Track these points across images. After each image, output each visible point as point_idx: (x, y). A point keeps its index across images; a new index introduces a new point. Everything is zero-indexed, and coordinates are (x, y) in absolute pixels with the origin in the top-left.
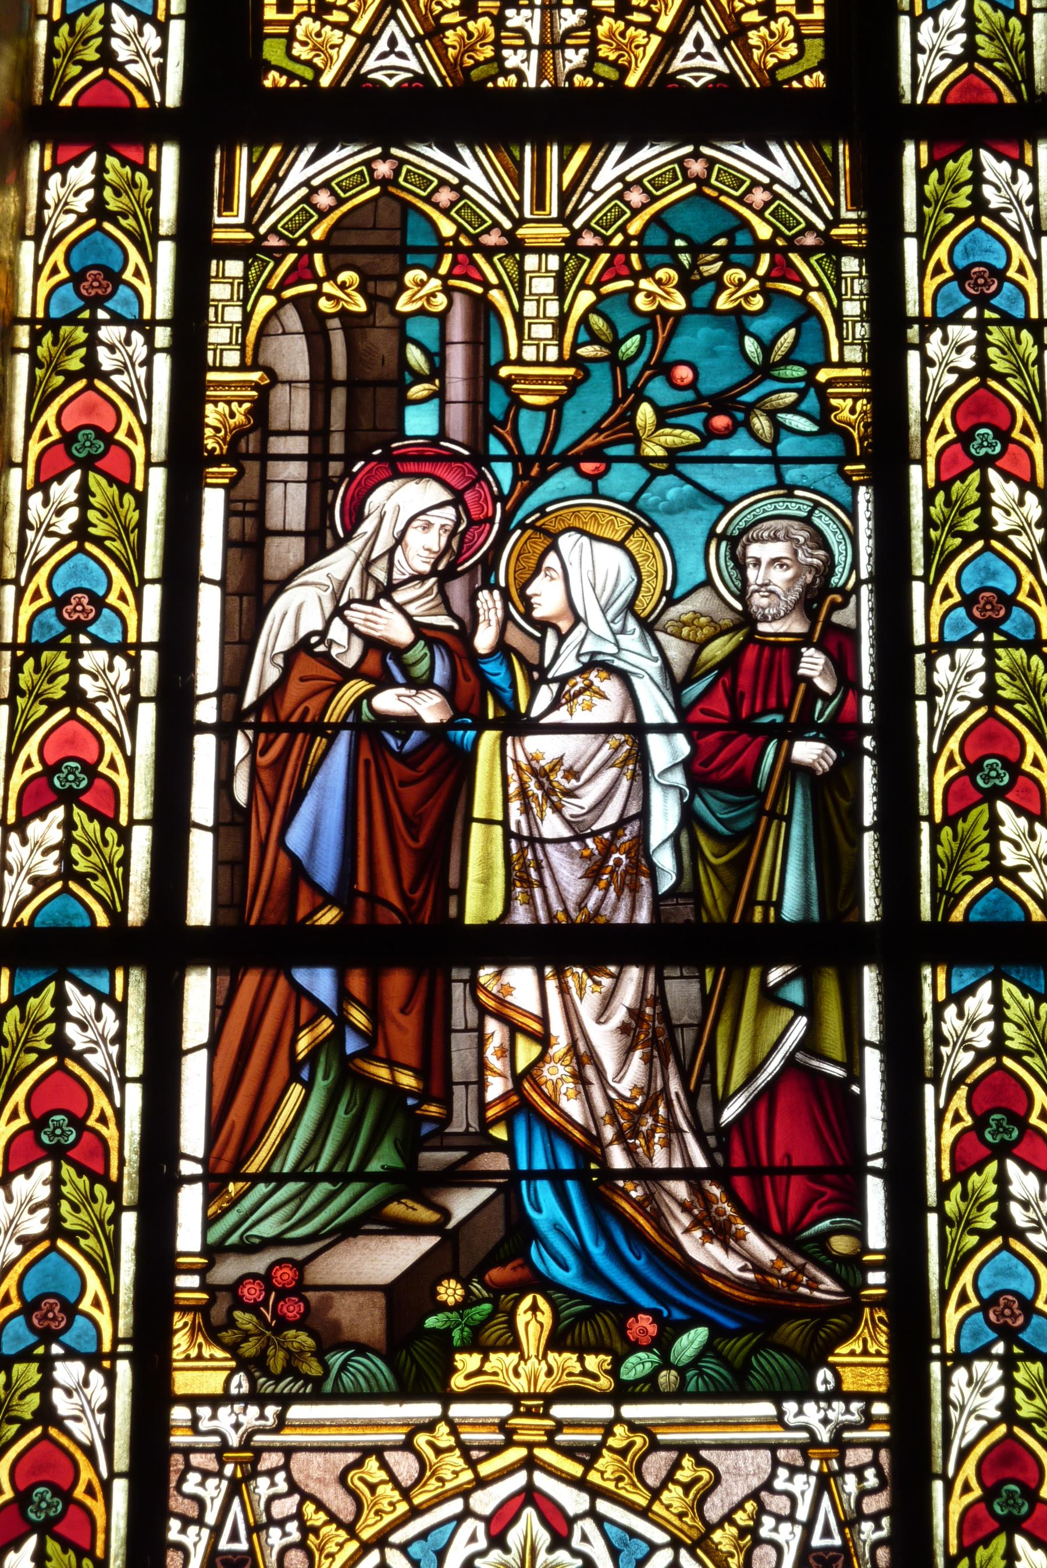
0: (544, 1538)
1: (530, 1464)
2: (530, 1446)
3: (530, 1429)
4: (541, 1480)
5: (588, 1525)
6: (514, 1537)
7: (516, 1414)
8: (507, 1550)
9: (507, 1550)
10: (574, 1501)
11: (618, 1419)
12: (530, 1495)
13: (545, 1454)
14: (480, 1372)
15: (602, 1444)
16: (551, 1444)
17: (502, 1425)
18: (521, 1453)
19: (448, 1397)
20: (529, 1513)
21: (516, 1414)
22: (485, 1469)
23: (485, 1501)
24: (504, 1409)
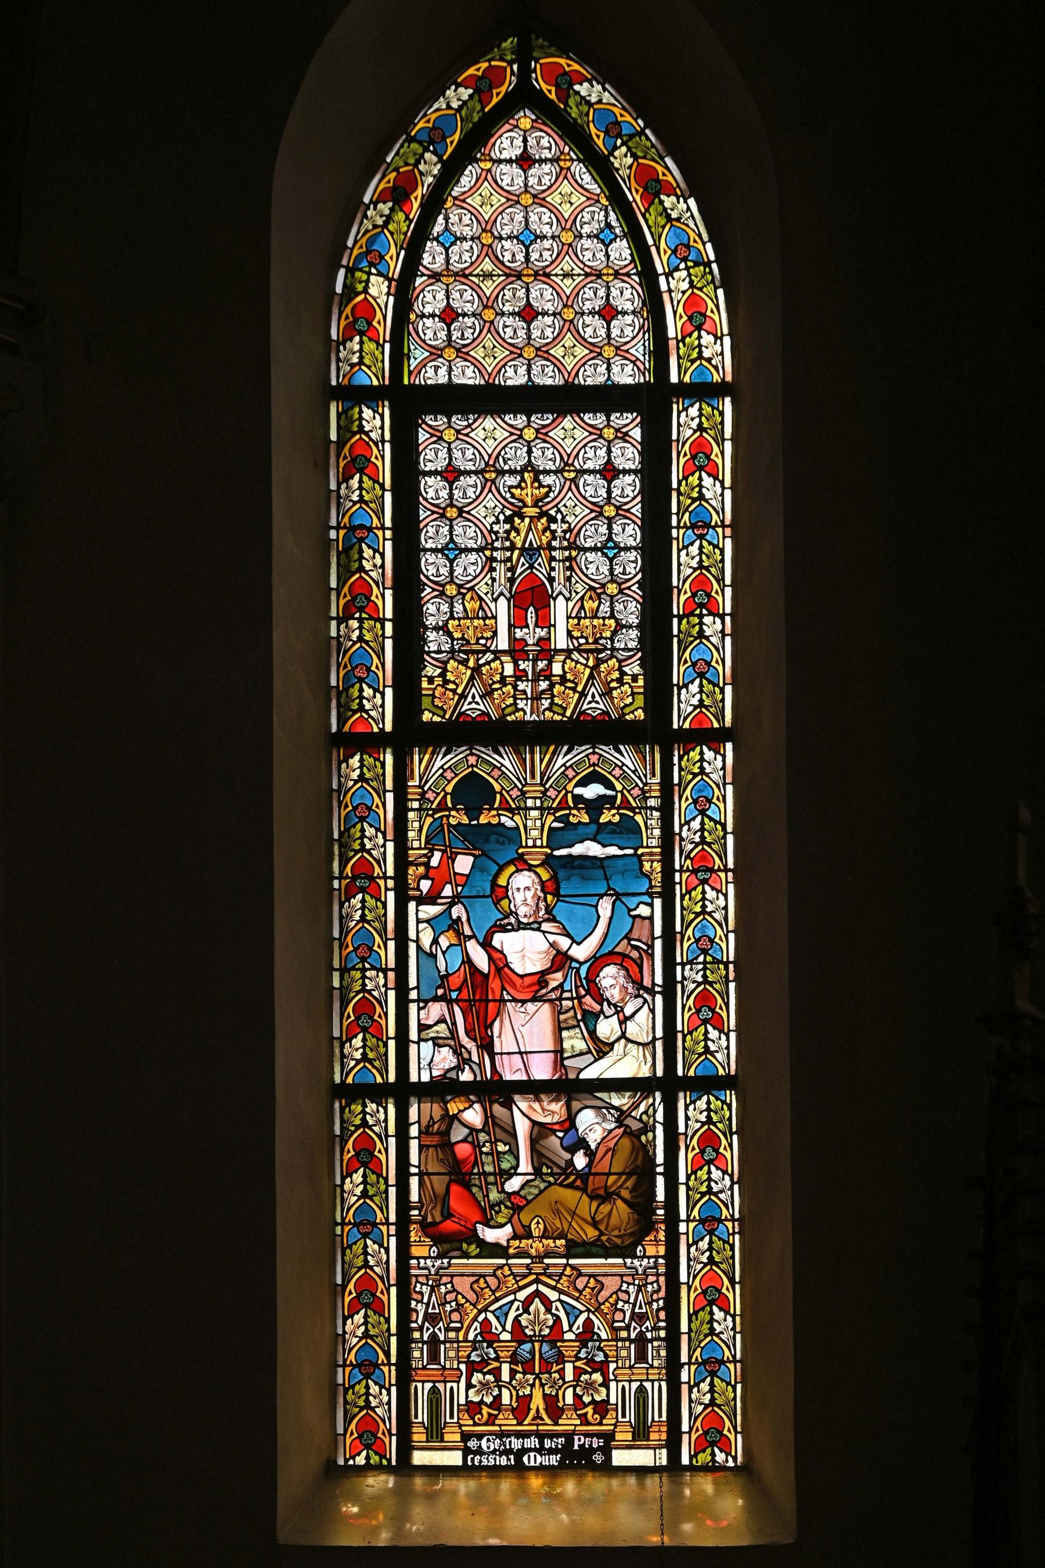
0: (542, 1309)
1: (537, 1281)
3: (538, 1269)
4: (542, 1288)
5: (558, 1304)
6: (532, 1309)
7: (532, 1263)
8: (529, 1314)
9: (529, 1314)
10: (553, 1295)
11: (567, 1264)
12: (537, 1293)
13: (544, 1278)
14: (518, 1247)
15: (562, 1274)
16: (545, 1274)
17: (527, 1266)
18: (534, 1277)
19: (508, 1257)
20: (537, 1300)
21: (532, 1263)
22: (521, 1284)
23: (522, 1295)
24: (528, 1261)
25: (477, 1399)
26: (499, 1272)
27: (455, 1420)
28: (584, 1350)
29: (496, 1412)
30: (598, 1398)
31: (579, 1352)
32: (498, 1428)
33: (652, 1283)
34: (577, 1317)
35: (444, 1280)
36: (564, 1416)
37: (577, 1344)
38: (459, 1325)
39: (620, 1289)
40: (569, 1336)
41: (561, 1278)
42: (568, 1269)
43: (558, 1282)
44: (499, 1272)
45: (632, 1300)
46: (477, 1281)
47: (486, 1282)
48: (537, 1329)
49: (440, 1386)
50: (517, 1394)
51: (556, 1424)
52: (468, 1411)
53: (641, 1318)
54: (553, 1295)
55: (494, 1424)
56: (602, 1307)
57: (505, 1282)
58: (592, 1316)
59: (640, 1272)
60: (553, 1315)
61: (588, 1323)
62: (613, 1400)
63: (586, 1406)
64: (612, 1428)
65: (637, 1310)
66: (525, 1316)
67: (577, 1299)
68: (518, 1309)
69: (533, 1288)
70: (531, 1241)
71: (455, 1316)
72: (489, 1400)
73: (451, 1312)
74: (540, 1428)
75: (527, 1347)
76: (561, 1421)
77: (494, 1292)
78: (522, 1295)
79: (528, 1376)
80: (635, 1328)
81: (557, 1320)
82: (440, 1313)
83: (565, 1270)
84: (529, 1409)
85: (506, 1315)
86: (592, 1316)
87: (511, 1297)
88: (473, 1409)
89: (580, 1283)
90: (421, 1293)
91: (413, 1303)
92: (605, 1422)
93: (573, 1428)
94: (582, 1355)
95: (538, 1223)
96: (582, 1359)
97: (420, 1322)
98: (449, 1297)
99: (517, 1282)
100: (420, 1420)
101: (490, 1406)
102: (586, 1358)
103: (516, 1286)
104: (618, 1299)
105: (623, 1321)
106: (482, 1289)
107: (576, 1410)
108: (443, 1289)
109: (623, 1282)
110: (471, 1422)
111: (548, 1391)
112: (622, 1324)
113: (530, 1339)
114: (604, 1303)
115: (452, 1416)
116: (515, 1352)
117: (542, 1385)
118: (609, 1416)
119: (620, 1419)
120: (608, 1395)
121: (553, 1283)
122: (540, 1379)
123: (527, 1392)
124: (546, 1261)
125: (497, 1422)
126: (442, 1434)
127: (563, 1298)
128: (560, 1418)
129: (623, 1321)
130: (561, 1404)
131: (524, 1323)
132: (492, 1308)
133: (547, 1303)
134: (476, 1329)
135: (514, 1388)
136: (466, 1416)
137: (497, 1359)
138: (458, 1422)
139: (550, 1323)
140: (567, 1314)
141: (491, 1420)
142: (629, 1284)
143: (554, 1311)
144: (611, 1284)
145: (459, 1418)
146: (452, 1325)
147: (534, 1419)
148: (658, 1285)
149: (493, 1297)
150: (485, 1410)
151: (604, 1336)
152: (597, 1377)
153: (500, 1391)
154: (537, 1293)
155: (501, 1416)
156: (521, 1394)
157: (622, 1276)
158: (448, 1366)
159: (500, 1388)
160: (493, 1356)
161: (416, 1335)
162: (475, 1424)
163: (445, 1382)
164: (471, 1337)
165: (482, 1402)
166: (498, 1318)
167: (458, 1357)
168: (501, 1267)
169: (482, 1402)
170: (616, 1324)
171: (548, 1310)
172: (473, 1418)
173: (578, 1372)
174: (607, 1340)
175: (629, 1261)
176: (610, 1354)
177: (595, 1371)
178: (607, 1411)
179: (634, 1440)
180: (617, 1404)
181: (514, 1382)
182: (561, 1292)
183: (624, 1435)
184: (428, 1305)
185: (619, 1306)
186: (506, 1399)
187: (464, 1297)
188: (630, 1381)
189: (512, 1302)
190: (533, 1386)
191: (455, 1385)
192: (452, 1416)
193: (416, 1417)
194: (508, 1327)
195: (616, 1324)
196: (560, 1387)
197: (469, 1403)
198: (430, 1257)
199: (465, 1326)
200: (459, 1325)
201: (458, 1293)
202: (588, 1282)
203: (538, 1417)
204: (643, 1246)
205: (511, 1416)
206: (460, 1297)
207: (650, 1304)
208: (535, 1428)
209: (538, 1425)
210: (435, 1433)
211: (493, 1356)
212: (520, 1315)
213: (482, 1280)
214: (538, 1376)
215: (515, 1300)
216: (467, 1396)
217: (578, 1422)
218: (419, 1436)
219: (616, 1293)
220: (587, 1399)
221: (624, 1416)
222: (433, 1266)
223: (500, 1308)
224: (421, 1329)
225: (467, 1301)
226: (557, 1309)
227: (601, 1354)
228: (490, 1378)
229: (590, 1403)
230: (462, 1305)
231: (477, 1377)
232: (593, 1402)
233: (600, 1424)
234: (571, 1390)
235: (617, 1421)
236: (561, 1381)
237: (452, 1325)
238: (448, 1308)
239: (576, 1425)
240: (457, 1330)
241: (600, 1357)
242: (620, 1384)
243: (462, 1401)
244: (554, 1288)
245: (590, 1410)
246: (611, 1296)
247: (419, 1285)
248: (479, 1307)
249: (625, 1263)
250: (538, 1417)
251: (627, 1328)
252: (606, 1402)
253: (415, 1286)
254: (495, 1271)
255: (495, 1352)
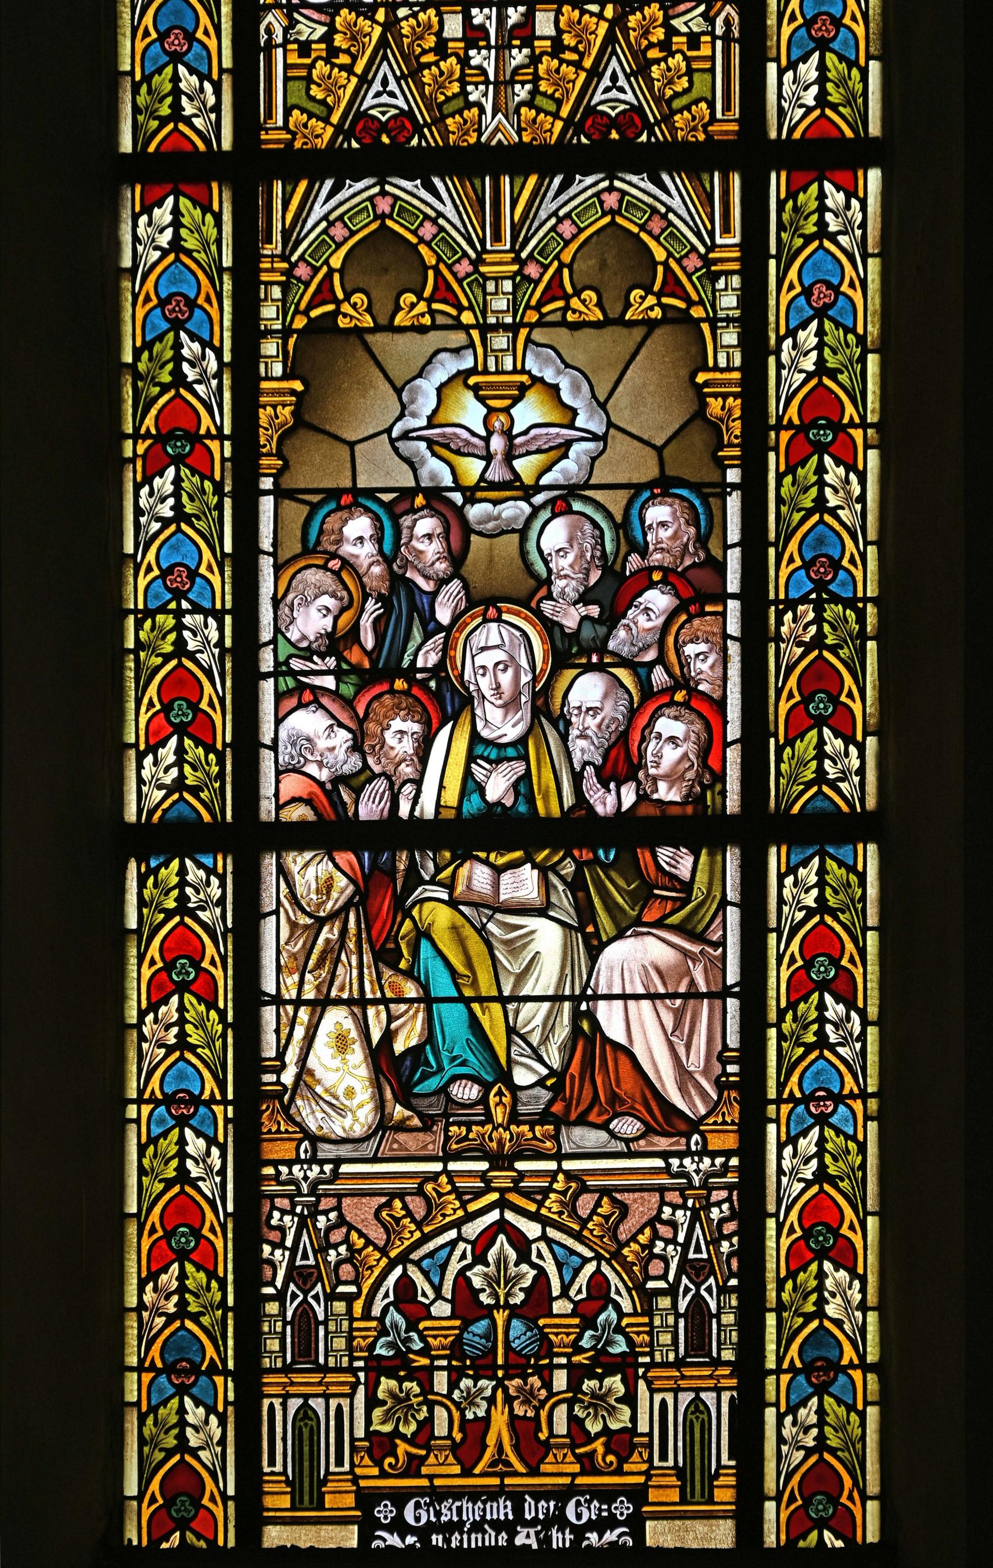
0: (512, 1255)
1: (502, 1204)
2: (502, 1191)
3: (502, 1178)
5: (542, 1246)
6: (492, 1255)
10: (532, 1230)
12: (502, 1226)
17: (483, 1176)
18: (494, 1196)
20: (502, 1238)
22: (472, 1207)
25: (387, 1428)
26: (429, 1187)
27: (347, 1467)
28: (589, 1333)
29: (423, 1452)
30: (614, 1426)
31: (580, 1337)
32: (425, 1482)
33: (719, 1204)
34: (577, 1272)
35: (325, 1204)
36: (550, 1458)
37: (576, 1321)
38: (353, 1289)
39: (658, 1218)
40: (560, 1306)
41: (546, 1197)
42: (561, 1177)
43: (541, 1204)
44: (429, 1187)
45: (681, 1238)
46: (388, 1205)
47: (405, 1207)
48: (501, 1293)
49: (317, 1404)
50: (463, 1415)
51: (534, 1471)
52: (369, 1451)
53: (696, 1270)
54: (532, 1230)
55: (418, 1475)
56: (625, 1251)
57: (443, 1206)
58: (605, 1269)
59: (697, 1182)
60: (533, 1266)
61: (598, 1280)
62: (643, 1427)
63: (590, 1439)
64: (641, 1479)
65: (691, 1255)
66: (479, 1268)
67: (578, 1237)
68: (463, 1256)
69: (494, 1215)
70: (489, 1127)
71: (346, 1271)
72: (409, 1429)
73: (339, 1263)
74: (508, 1481)
75: (481, 1326)
76: (544, 1468)
77: (419, 1225)
78: (473, 1229)
79: (483, 1383)
80: (687, 1290)
81: (542, 1274)
82: (317, 1266)
83: (554, 1180)
84: (485, 1447)
85: (444, 1267)
86: (605, 1269)
87: (453, 1234)
88: (380, 1445)
89: (585, 1203)
90: (282, 1230)
91: (267, 1249)
92: (626, 1467)
93: (567, 1480)
94: (585, 1343)
95: (500, 1093)
96: (585, 1351)
97: (279, 1283)
98: (336, 1236)
99: (464, 1205)
100: (278, 1468)
101: (411, 1441)
102: (593, 1348)
103: (460, 1213)
104: (656, 1236)
105: (664, 1277)
106: (397, 1220)
107: (573, 1447)
108: (322, 1222)
109: (663, 1203)
110: (375, 1471)
111: (519, 1410)
112: (662, 1284)
113: (487, 1312)
114: (627, 1244)
115: (339, 1462)
116: (459, 1338)
117: (509, 1400)
118: (636, 1457)
119: (656, 1463)
120: (634, 1419)
121: (532, 1207)
122: (505, 1390)
123: (481, 1413)
124: (521, 1165)
125: (424, 1470)
126: (321, 1496)
127: (551, 1233)
128: (542, 1461)
129: (664, 1277)
130: (543, 1436)
131: (477, 1282)
132: (415, 1256)
133: (521, 1244)
134: (386, 1295)
135: (457, 1405)
136: (367, 1461)
137: (425, 1352)
138: (351, 1472)
139: (527, 1283)
140: (559, 1266)
141: (413, 1467)
142: (675, 1207)
143: (534, 1258)
144: (642, 1207)
145: (352, 1465)
146: (341, 1289)
147: (493, 1464)
148: (732, 1208)
149: (417, 1235)
150: (402, 1447)
151: (626, 1306)
152: (615, 1383)
153: (431, 1411)
154: (502, 1226)
155: (432, 1460)
156: (470, 1416)
157: (662, 1190)
158: (332, 1363)
159: (431, 1405)
160: (418, 1345)
161: (272, 1308)
162: (383, 1475)
163: (327, 1397)
164: (376, 1311)
165: (396, 1433)
166: (426, 1274)
167: (350, 1348)
168: (434, 1177)
169: (396, 1433)
170: (651, 1285)
171: (524, 1257)
172: (378, 1463)
173: (577, 1375)
174: (635, 1314)
175: (675, 1162)
176: (638, 1339)
177: (610, 1372)
178: (633, 1447)
179: (683, 1501)
180: (650, 1435)
181: (456, 1395)
182: (545, 1222)
183: (665, 1493)
184: (294, 1250)
185: (656, 1251)
186: (441, 1429)
187: (361, 1235)
188: (676, 1391)
189: (453, 1244)
190: (491, 1401)
191: (345, 1403)
192: (339, 1462)
193: (272, 1463)
194: (447, 1291)
195: (651, 1285)
196: (543, 1403)
197: (369, 1435)
198: (298, 1160)
199: (365, 1291)
200: (353, 1289)
201: (351, 1227)
202: (598, 1204)
203: (501, 1456)
204: (702, 1134)
205: (451, 1459)
206: (354, 1235)
207: (715, 1242)
208: (495, 1481)
209: (502, 1475)
210: (308, 1493)
211: (418, 1345)
212: (469, 1267)
213: (397, 1204)
214: (500, 1384)
215: (460, 1238)
216: (368, 1422)
217: (576, 1468)
218: (277, 1500)
219: (651, 1223)
220: (594, 1427)
221: (664, 1457)
222: (306, 1178)
223: (431, 1255)
224: (280, 1297)
225: (369, 1242)
226: (540, 1255)
227: (620, 1338)
228: (413, 1387)
229: (598, 1435)
230: (359, 1251)
231: (387, 1384)
232: (606, 1431)
233: (619, 1472)
234: (564, 1407)
235: (652, 1467)
236: (543, 1393)
237: (341, 1289)
238: (332, 1256)
239: (574, 1476)
240: (349, 1299)
241: (620, 1347)
242: (658, 1398)
243: (360, 1433)
244: (533, 1217)
245: (599, 1446)
246: (641, 1231)
247: (276, 1215)
248: (393, 1254)
249: (669, 1165)
250: (501, 1456)
251: (672, 1292)
252: (632, 1431)
253: (270, 1217)
254: (421, 1185)
255: (423, 1338)
